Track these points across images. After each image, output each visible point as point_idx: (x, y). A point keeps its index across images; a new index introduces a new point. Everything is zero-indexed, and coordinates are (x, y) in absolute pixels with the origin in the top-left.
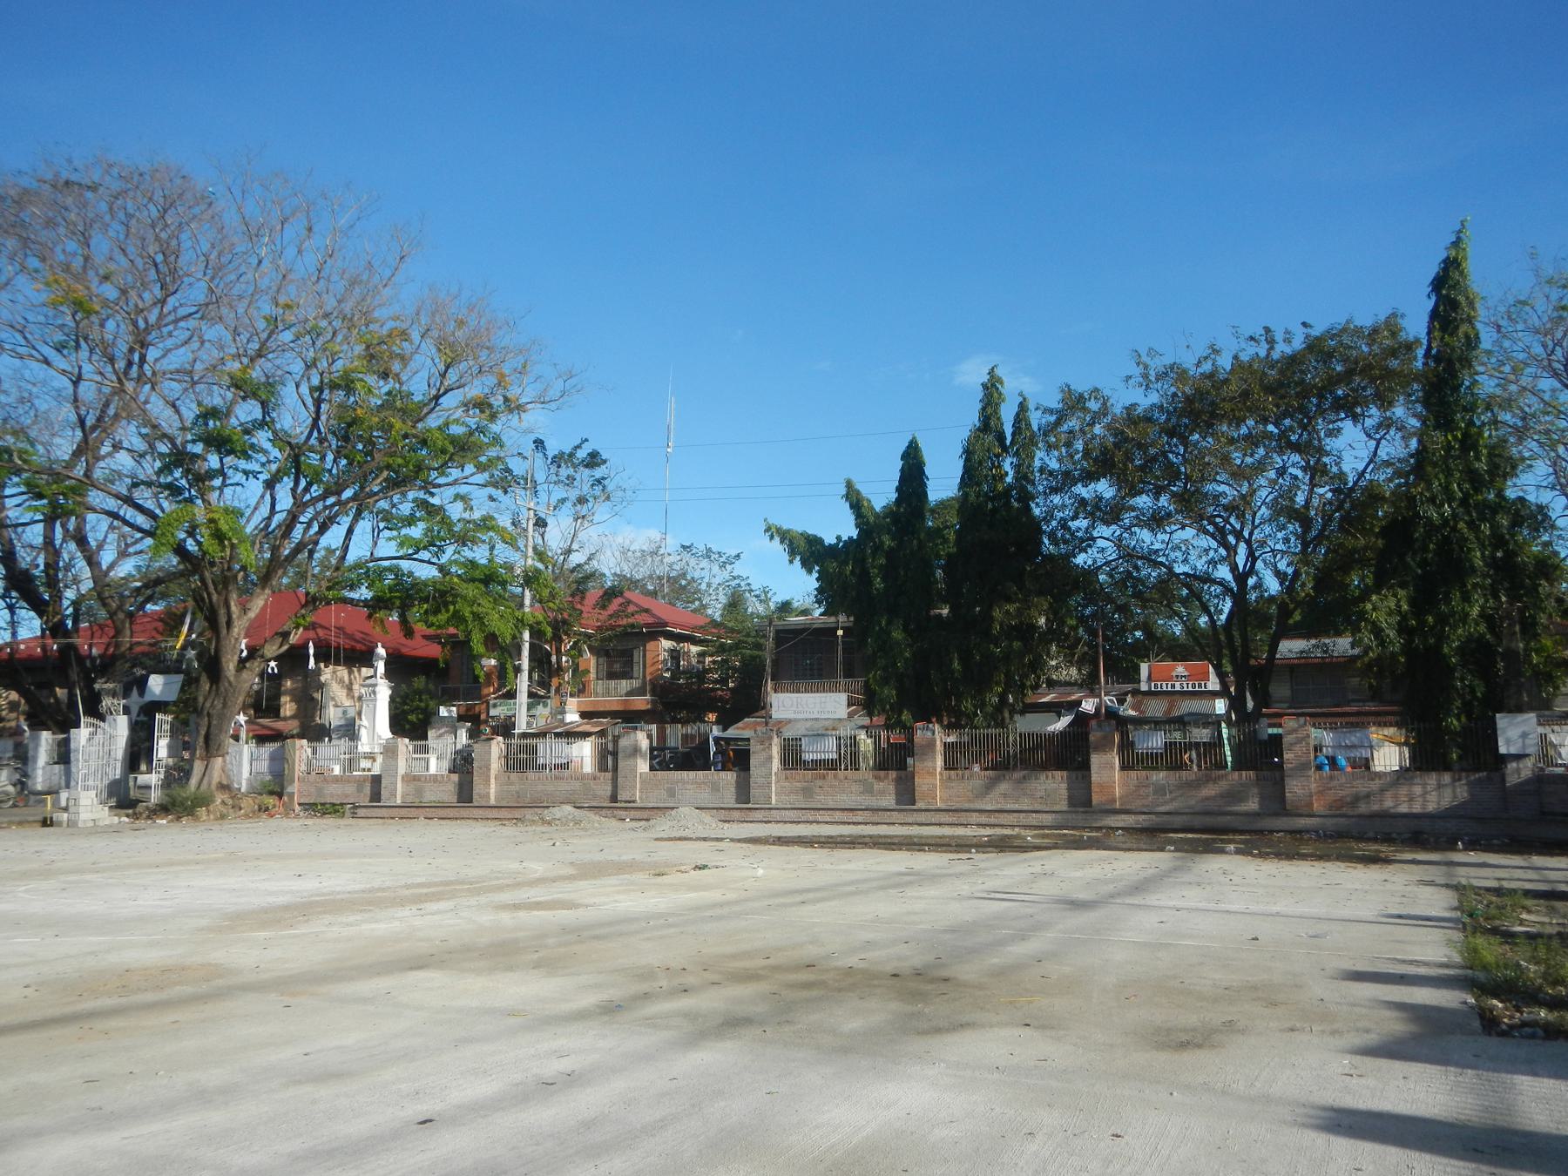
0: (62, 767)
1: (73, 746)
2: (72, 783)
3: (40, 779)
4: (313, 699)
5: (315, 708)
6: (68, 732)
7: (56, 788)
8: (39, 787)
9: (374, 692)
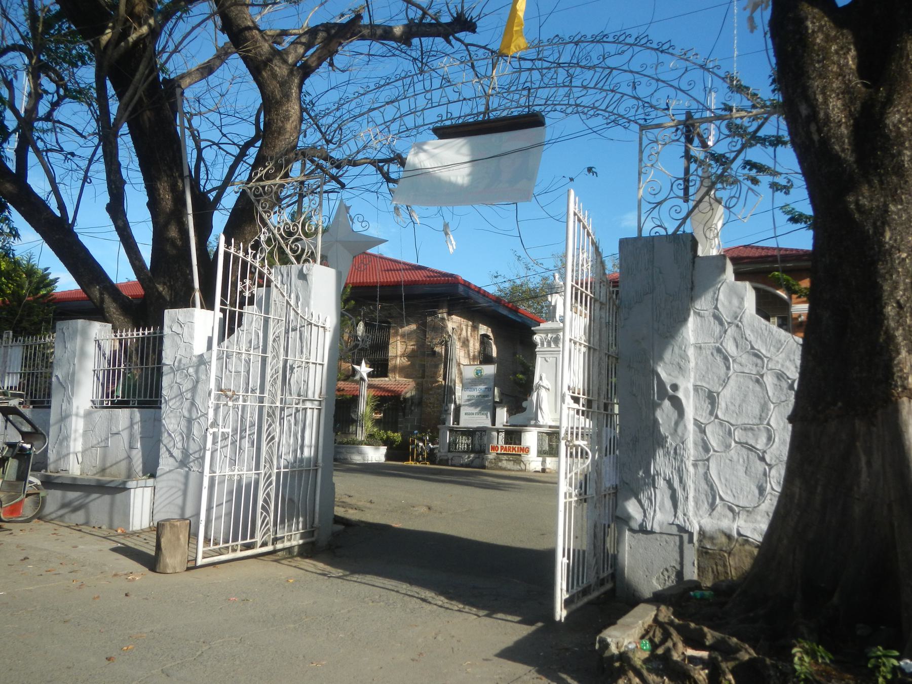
0: (137, 413)
1: (168, 356)
2: (165, 463)
3: (77, 445)
4: (434, 353)
5: (437, 366)
6: (160, 322)
7: (116, 474)
8: (74, 468)
9: (556, 341)
